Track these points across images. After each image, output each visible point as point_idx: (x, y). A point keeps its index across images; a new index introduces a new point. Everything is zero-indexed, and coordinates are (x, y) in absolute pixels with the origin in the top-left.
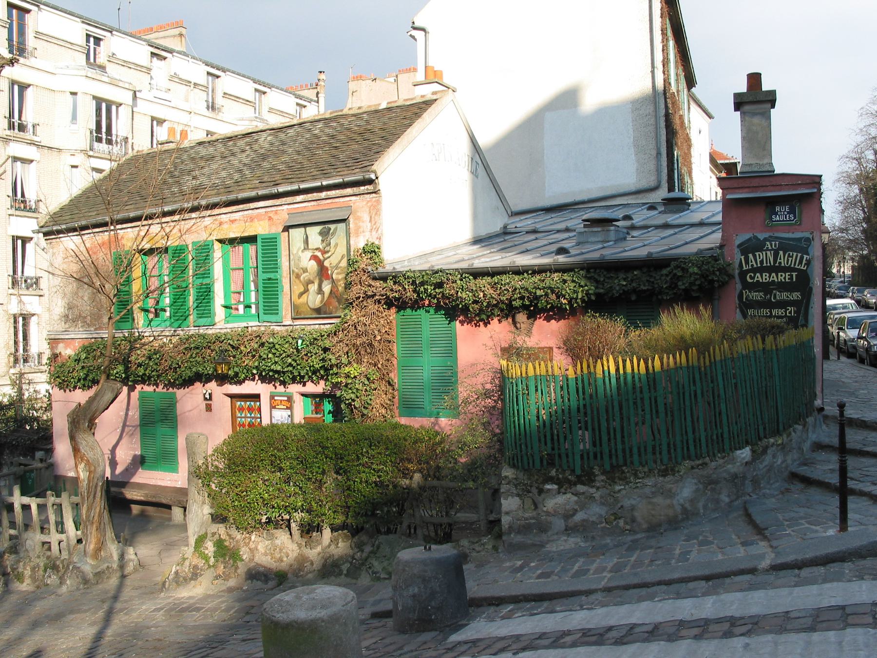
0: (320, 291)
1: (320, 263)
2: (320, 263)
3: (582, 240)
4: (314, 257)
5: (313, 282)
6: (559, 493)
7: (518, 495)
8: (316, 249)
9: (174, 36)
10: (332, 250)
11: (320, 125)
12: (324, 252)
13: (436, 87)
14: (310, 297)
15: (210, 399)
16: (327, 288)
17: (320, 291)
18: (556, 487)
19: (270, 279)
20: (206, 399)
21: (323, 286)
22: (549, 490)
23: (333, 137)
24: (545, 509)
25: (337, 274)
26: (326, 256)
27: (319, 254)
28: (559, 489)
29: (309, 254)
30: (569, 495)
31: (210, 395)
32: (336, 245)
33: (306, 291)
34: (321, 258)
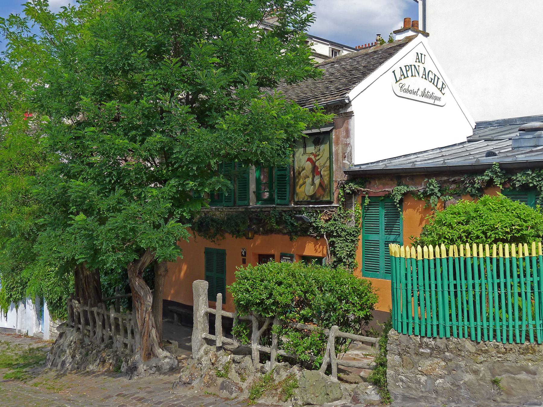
0: (313, 183)
1: (313, 163)
2: (313, 163)
3: (516, 146)
4: (309, 160)
5: (309, 177)
7: (399, 354)
8: (312, 153)
10: (321, 154)
11: (328, 66)
12: (316, 156)
13: (410, 33)
14: (306, 187)
15: (245, 256)
16: (317, 181)
17: (313, 183)
19: (282, 175)
20: (242, 255)
21: (315, 179)
22: (423, 353)
23: (332, 74)
24: (420, 368)
25: (324, 171)
26: (317, 158)
27: (312, 157)
28: (431, 354)
29: (306, 157)
30: (436, 360)
31: (245, 252)
32: (324, 150)
33: (304, 183)
34: (314, 160)
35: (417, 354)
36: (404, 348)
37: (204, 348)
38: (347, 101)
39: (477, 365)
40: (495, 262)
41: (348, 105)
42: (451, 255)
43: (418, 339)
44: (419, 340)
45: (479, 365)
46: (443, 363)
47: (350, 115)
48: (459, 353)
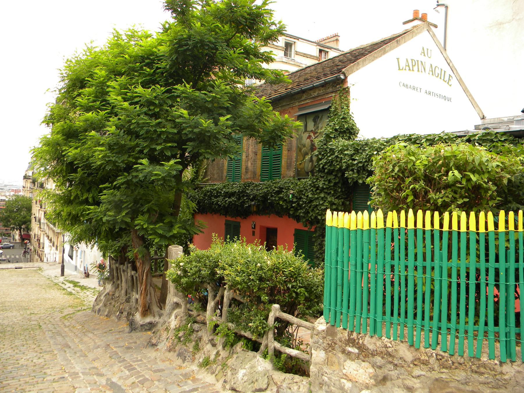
6: (358, 358)
7: (325, 350)
9: (334, 41)
18: (356, 351)
24: (344, 371)
35: (343, 351)
36: (330, 343)
37: (175, 312)
38: (342, 77)
39: (413, 379)
40: (445, 237)
41: (344, 81)
42: (389, 225)
43: (346, 334)
44: (346, 335)
45: (415, 380)
46: (371, 370)
47: (347, 91)
48: (390, 359)
